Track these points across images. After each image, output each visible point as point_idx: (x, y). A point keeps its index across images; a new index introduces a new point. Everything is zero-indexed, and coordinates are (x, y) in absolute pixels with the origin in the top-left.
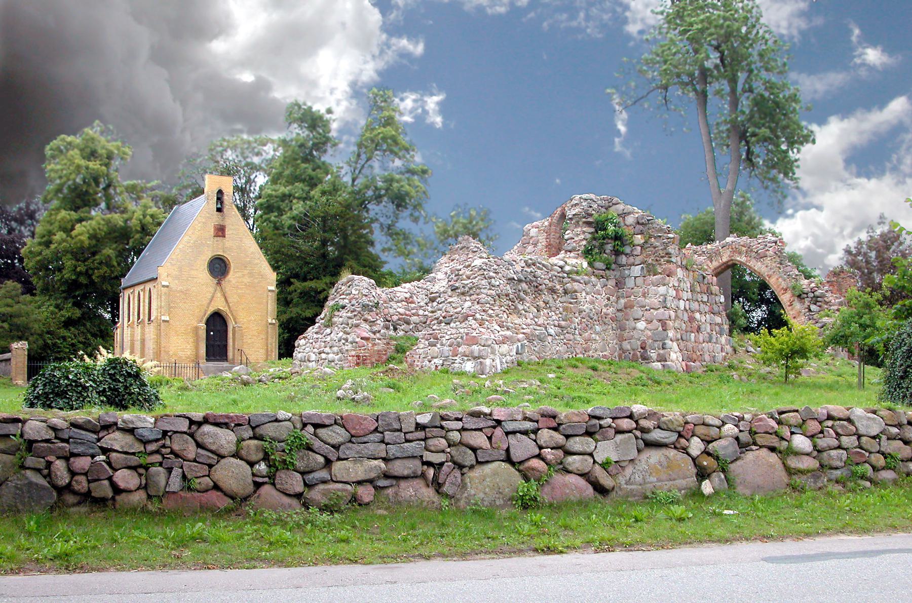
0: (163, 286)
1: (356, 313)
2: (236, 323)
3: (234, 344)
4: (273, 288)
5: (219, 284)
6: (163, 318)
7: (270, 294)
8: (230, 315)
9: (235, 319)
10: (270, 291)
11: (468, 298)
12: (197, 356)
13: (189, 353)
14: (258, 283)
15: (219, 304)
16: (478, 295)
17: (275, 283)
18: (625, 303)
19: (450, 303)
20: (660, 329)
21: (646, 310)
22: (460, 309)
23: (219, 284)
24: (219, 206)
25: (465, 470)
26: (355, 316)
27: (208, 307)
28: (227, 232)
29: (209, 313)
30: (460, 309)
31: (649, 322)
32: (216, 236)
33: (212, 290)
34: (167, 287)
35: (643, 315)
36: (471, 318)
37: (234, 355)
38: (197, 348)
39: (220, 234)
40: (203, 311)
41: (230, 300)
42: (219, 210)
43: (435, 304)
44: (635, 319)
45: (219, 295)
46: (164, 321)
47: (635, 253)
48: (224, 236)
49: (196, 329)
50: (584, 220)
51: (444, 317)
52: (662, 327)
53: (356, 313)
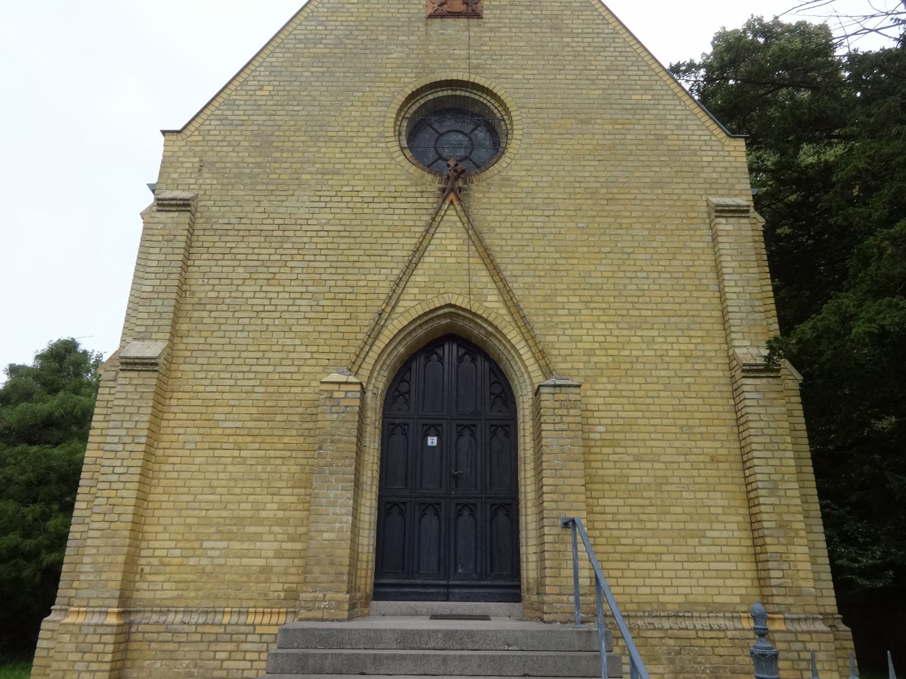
2: (548, 371)
7: (725, 225)
8: (513, 336)
9: (541, 355)
10: (724, 211)
13: (268, 547)
40: (366, 319)
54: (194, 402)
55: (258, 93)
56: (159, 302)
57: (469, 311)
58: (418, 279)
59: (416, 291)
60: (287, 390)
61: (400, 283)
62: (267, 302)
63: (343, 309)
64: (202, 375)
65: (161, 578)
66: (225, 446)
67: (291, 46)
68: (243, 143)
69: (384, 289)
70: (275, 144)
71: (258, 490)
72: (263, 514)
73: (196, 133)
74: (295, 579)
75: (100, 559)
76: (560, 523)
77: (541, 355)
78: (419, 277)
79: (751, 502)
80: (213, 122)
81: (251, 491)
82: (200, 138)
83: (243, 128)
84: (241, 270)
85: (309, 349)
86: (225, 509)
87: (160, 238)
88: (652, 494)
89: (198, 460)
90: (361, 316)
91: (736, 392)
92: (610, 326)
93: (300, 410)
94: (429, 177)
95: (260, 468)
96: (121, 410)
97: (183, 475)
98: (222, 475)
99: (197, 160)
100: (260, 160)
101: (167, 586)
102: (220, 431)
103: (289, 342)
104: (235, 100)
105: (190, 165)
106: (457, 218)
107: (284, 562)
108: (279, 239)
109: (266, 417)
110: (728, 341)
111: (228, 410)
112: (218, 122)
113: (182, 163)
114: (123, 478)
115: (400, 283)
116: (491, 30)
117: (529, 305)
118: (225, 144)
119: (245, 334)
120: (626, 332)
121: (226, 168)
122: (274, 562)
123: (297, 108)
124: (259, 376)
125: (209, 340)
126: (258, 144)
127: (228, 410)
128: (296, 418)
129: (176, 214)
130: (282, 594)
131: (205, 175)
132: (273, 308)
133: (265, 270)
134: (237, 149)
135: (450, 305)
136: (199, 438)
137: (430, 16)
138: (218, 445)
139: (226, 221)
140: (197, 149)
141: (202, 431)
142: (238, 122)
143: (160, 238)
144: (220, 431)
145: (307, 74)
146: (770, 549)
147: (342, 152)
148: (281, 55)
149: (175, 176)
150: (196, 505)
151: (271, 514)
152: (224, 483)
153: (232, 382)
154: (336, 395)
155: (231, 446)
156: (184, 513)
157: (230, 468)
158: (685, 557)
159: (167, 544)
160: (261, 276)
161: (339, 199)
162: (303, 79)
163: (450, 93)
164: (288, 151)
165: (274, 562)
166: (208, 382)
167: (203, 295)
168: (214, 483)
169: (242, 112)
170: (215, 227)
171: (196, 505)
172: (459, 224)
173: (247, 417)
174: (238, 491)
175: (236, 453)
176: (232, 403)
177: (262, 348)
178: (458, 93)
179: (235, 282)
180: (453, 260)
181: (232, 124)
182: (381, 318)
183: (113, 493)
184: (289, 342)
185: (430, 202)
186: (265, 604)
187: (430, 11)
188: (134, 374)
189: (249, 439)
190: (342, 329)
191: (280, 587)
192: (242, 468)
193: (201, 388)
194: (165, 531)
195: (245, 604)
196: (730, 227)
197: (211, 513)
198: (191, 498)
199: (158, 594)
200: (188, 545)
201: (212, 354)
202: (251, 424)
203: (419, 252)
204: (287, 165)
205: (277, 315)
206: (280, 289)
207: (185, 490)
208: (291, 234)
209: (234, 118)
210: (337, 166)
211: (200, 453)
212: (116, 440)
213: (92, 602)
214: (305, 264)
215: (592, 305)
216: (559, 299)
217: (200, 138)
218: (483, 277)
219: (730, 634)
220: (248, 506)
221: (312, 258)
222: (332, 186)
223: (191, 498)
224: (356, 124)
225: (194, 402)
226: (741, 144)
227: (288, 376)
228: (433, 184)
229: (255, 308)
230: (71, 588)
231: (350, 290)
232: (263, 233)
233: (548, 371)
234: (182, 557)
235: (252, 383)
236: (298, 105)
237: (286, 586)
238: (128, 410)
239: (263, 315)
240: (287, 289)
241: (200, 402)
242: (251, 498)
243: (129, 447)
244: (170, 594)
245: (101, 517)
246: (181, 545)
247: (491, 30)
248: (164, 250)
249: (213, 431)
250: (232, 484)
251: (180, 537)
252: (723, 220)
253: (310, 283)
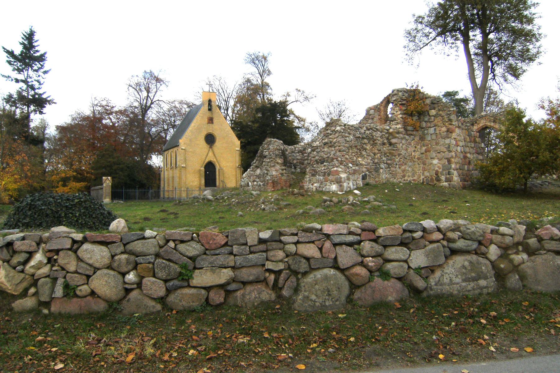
0: (182, 149)
1: (272, 159)
2: (220, 167)
3: (219, 178)
4: (238, 149)
5: (211, 147)
9: (219, 165)
10: (237, 150)
11: (333, 149)
12: (200, 184)
15: (211, 158)
16: (340, 146)
17: (239, 147)
18: (426, 150)
19: (323, 152)
20: (447, 163)
21: (438, 153)
22: (329, 155)
23: (211, 147)
24: (210, 108)
25: (300, 276)
26: (272, 161)
27: (205, 159)
28: (215, 121)
29: (206, 162)
30: (329, 155)
31: (440, 159)
32: (209, 123)
33: (207, 151)
34: (184, 149)
35: (436, 156)
36: (335, 160)
37: (219, 183)
38: (200, 180)
39: (211, 122)
40: (203, 162)
41: (217, 156)
42: (210, 110)
43: (315, 153)
44: (431, 158)
45: (211, 154)
46: (183, 167)
47: (431, 120)
48: (212, 123)
49: (200, 170)
50: (400, 103)
51: (320, 160)
52: (448, 162)
53: (272, 159)
61: (206, 158)
69: (204, 158)
77: (219, 165)
78: (208, 157)
79: (236, 179)
115: (206, 158)
117: (218, 160)
182: (204, 162)
203: (208, 154)
226: (239, 142)
228: (209, 146)
233: (220, 167)
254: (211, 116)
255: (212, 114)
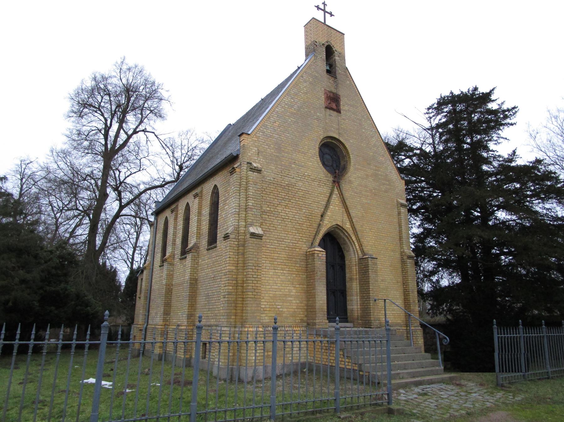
2: (362, 251)
6: (252, 230)
12: (310, 309)
14: (386, 191)
24: (328, 68)
28: (344, 106)
33: (326, 190)
34: (259, 171)
38: (310, 294)
39: (334, 106)
41: (353, 212)
42: (328, 72)
46: (253, 235)
54: (267, 251)
55: (274, 124)
56: (255, 210)
57: (342, 228)
58: (329, 213)
59: (328, 218)
60: (295, 249)
62: (286, 215)
63: (308, 221)
64: (268, 241)
65: (264, 315)
66: (278, 269)
67: (283, 105)
68: (271, 146)
70: (282, 149)
71: (290, 285)
72: (292, 294)
73: (255, 136)
74: (302, 316)
75: (253, 308)
76: (373, 300)
77: (361, 245)
78: (329, 213)
80: (260, 133)
81: (288, 285)
82: (256, 139)
83: (271, 139)
84: (276, 200)
85: (300, 235)
86: (280, 291)
87: (252, 183)
88: (385, 291)
89: (271, 273)
90: (314, 225)
91: (403, 262)
92: (376, 238)
93: (299, 257)
94: (329, 175)
95: (289, 277)
96: (252, 253)
97: (267, 279)
98: (279, 279)
99: (256, 149)
100: (278, 154)
101: (266, 318)
102: (276, 263)
103: (294, 231)
104: (267, 125)
105: (254, 151)
106: (337, 193)
107: (299, 310)
108: (287, 190)
109: (290, 259)
110: (402, 248)
111: (278, 255)
112: (262, 134)
113: (252, 149)
114: (257, 279)
116: (344, 119)
117: (358, 227)
118: (265, 144)
119: (280, 227)
120: (379, 241)
121: (267, 155)
122: (296, 310)
123: (288, 135)
124: (286, 243)
125: (270, 228)
126: (277, 147)
127: (278, 255)
128: (298, 260)
129: (256, 174)
130: (300, 321)
131: (260, 157)
132: (287, 218)
133: (284, 202)
134: (270, 148)
135: (337, 225)
136: (270, 265)
137: (326, 108)
138: (276, 268)
139: (269, 178)
140: (256, 144)
141: (271, 262)
142: (269, 136)
143: (252, 183)
144: (276, 263)
145: (290, 120)
146: (412, 308)
147: (303, 158)
148: (280, 108)
149: (250, 154)
150: (271, 290)
151: (294, 294)
152: (279, 282)
153: (278, 245)
154: (320, 255)
155: (280, 269)
156: (269, 292)
157: (281, 277)
158: (391, 310)
159: (265, 303)
160: (283, 204)
161: (304, 177)
162: (289, 122)
163: (331, 141)
164: (287, 153)
165: (296, 310)
166: (270, 244)
167: (265, 209)
168: (277, 282)
169: (269, 131)
170: (266, 180)
171: (271, 290)
172: (338, 195)
173: (284, 259)
174: (284, 285)
175: (282, 272)
176: (279, 252)
177: (286, 233)
178: (333, 141)
179: (275, 205)
180: (337, 208)
181: (266, 136)
183: (254, 285)
184: (294, 231)
185: (330, 184)
186: (295, 324)
187: (326, 105)
188: (255, 240)
189: (285, 267)
190: (309, 229)
191: (298, 318)
192: (284, 277)
193: (269, 246)
194: (263, 299)
195: (289, 324)
196: (403, 211)
197: (277, 293)
198: (270, 287)
199: (264, 321)
200: (271, 304)
201: (271, 233)
202: (285, 261)
204: (287, 159)
205: (289, 220)
206: (289, 210)
207: (268, 284)
208: (290, 188)
209: (267, 133)
210: (303, 164)
211: (271, 271)
212: (252, 265)
213: (253, 324)
214: (296, 202)
215: (372, 230)
216: (364, 227)
217: (256, 139)
218: (346, 217)
219: (401, 331)
220: (287, 291)
221: (298, 200)
222: (302, 172)
223: (270, 287)
224: (306, 147)
225: (267, 251)
227: (295, 244)
229: (283, 217)
230: (231, 318)
231: (310, 214)
232: (282, 186)
233: (362, 251)
234: (269, 308)
235: (284, 246)
236: (288, 134)
237: (300, 318)
238: (255, 253)
239: (285, 220)
240: (292, 211)
241: (269, 251)
242: (288, 288)
243: (257, 268)
244: (267, 321)
245: (251, 293)
246: (269, 304)
247: (344, 119)
248: (254, 188)
249: (274, 263)
250: (282, 283)
251: (268, 301)
252: (402, 208)
253: (298, 210)
254: (334, 90)
255: (337, 87)
